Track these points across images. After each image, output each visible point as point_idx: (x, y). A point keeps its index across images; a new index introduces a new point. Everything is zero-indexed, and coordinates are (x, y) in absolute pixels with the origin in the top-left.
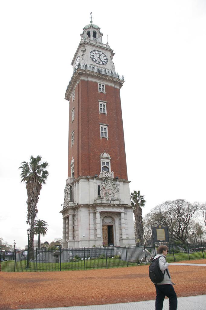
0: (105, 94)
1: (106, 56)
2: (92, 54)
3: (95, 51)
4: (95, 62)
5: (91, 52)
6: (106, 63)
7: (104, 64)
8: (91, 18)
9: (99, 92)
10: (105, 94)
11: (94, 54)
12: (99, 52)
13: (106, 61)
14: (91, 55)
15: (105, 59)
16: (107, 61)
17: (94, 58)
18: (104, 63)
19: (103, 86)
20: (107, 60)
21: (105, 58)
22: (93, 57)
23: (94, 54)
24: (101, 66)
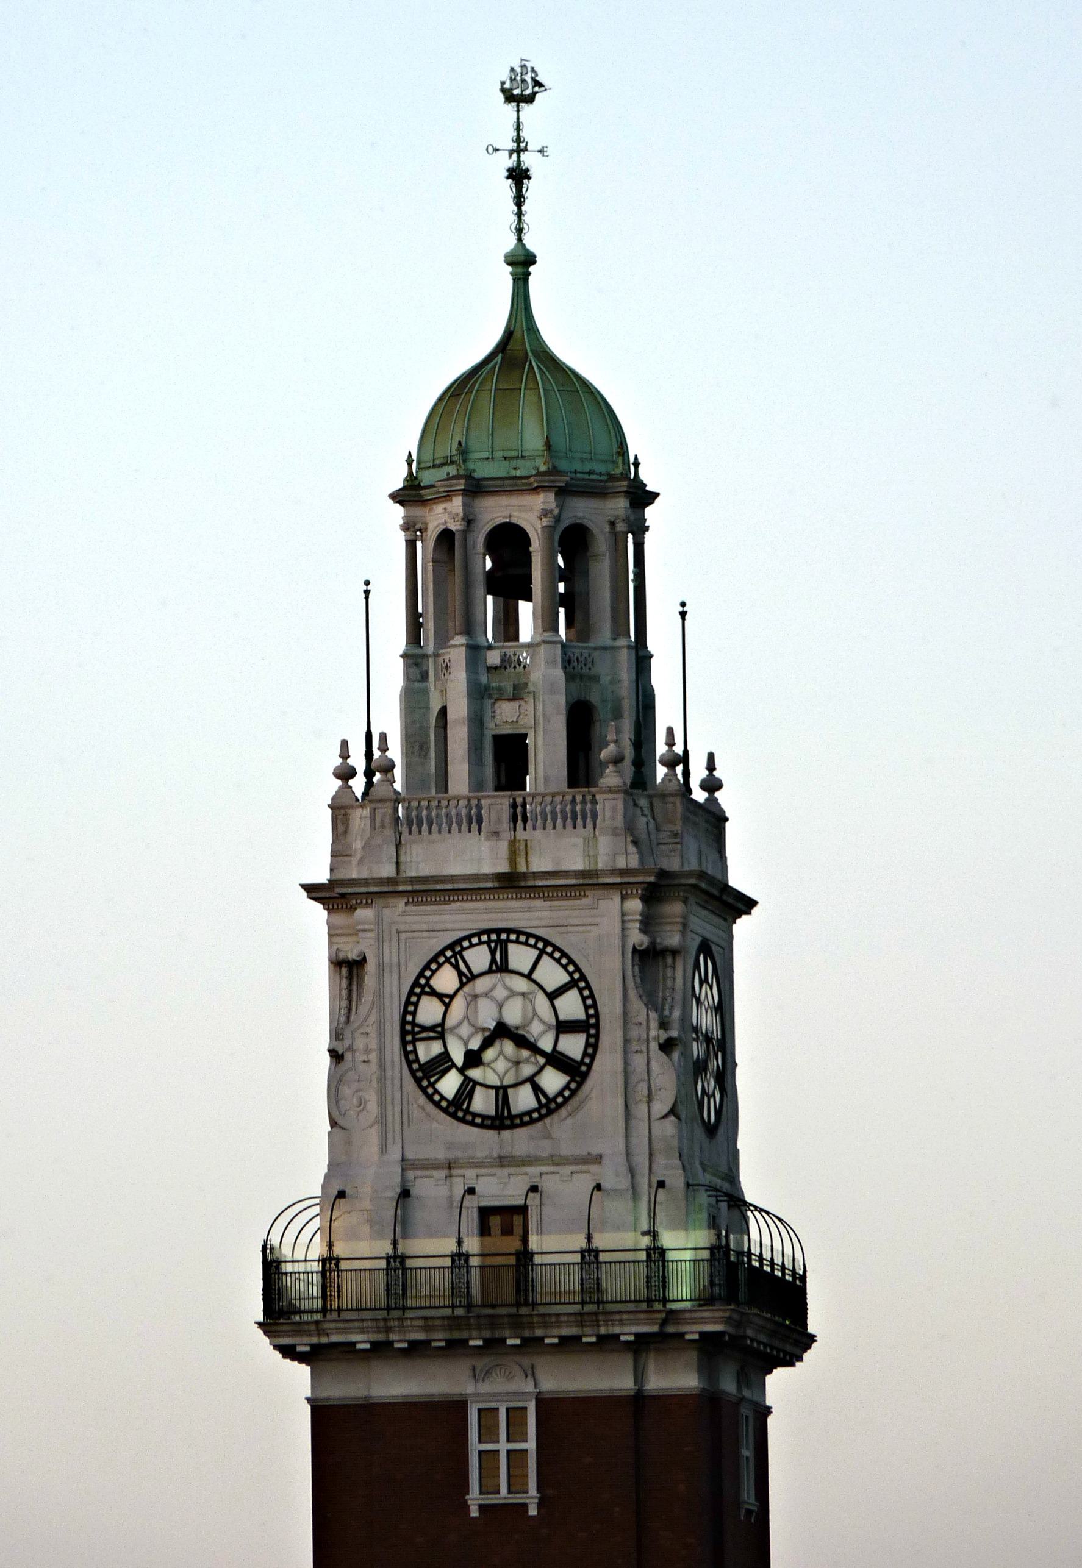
0: (533, 1511)
1: (578, 981)
2: (429, 1012)
3: (452, 954)
4: (457, 1108)
5: (421, 987)
6: (577, 1071)
7: (548, 1106)
8: (519, 176)
9: (474, 1513)
10: (533, 1511)
11: (446, 1000)
12: (499, 941)
13: (573, 1046)
14: (411, 1032)
15: (564, 1027)
16: (592, 1047)
17: (443, 1063)
18: (553, 1081)
19: (516, 1416)
20: (588, 1027)
21: (571, 1006)
22: (436, 1048)
23: (446, 1000)
24: (519, 1141)
